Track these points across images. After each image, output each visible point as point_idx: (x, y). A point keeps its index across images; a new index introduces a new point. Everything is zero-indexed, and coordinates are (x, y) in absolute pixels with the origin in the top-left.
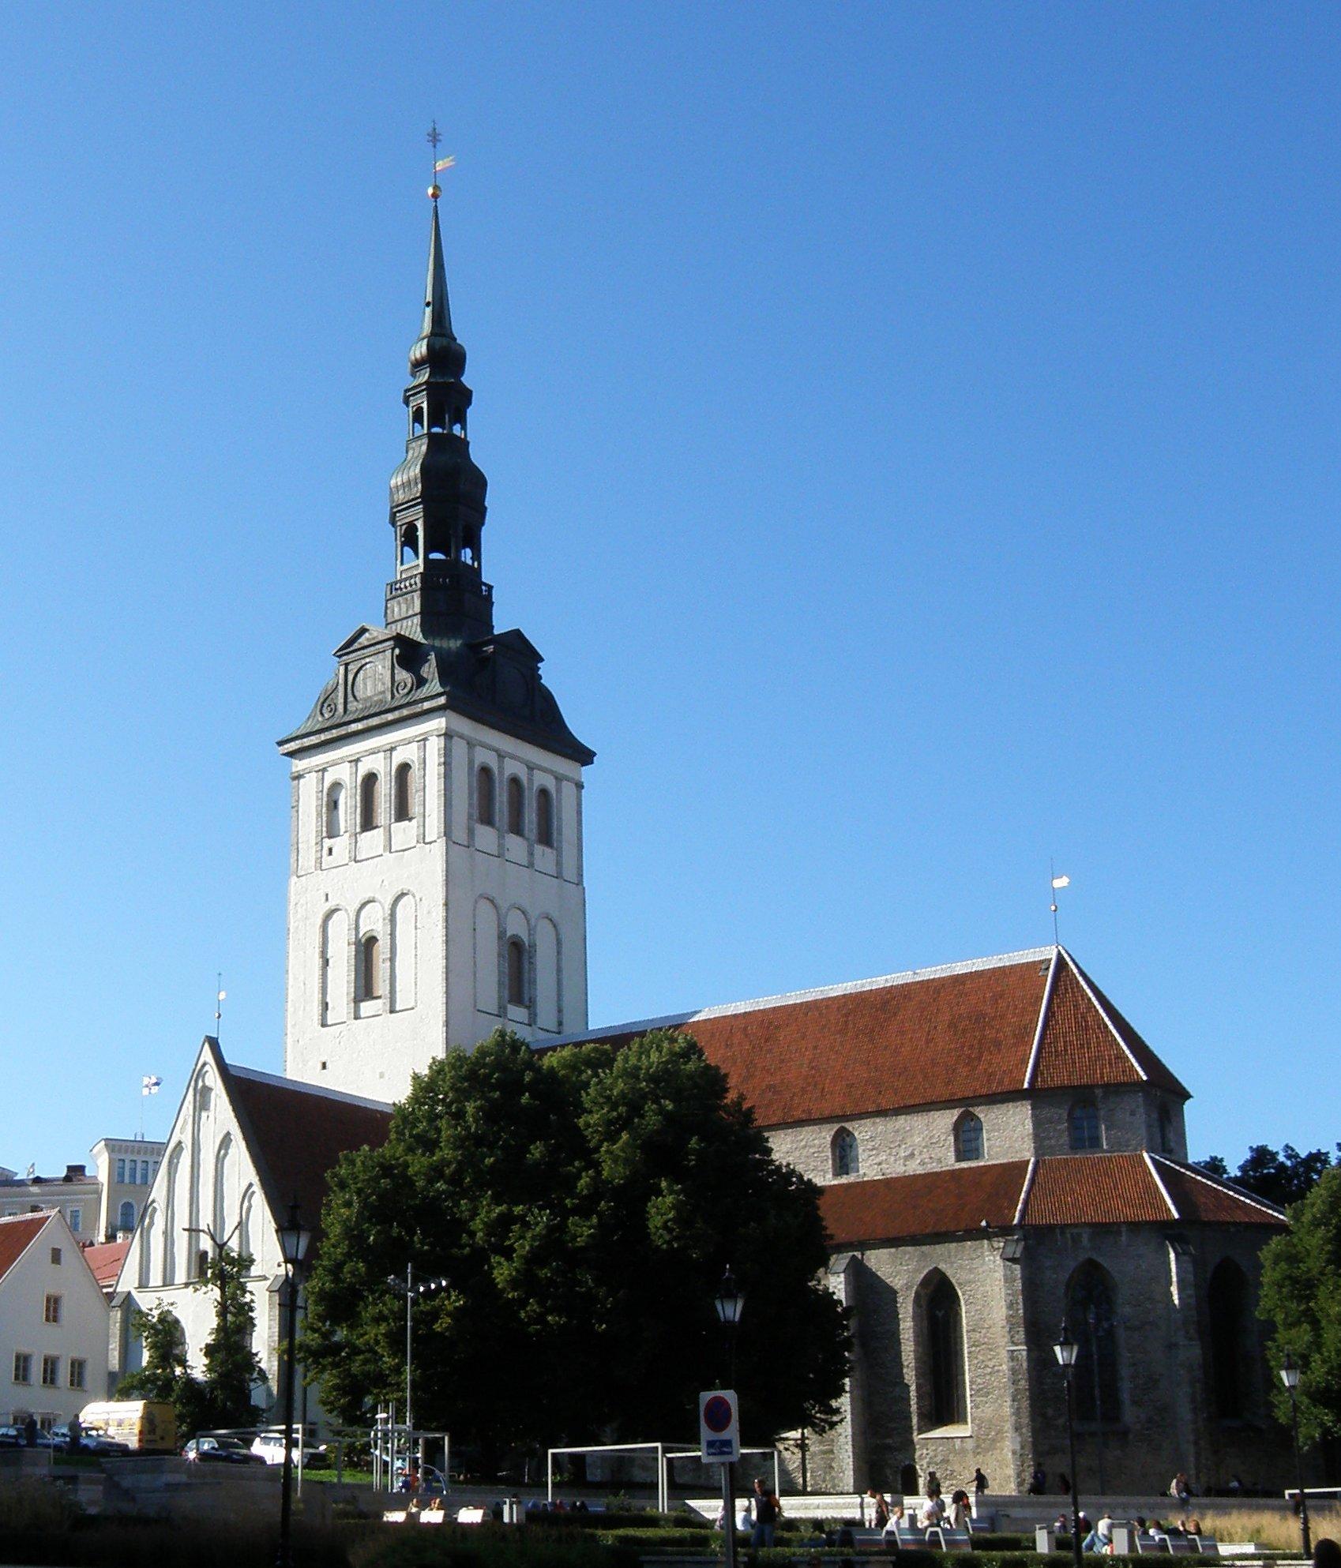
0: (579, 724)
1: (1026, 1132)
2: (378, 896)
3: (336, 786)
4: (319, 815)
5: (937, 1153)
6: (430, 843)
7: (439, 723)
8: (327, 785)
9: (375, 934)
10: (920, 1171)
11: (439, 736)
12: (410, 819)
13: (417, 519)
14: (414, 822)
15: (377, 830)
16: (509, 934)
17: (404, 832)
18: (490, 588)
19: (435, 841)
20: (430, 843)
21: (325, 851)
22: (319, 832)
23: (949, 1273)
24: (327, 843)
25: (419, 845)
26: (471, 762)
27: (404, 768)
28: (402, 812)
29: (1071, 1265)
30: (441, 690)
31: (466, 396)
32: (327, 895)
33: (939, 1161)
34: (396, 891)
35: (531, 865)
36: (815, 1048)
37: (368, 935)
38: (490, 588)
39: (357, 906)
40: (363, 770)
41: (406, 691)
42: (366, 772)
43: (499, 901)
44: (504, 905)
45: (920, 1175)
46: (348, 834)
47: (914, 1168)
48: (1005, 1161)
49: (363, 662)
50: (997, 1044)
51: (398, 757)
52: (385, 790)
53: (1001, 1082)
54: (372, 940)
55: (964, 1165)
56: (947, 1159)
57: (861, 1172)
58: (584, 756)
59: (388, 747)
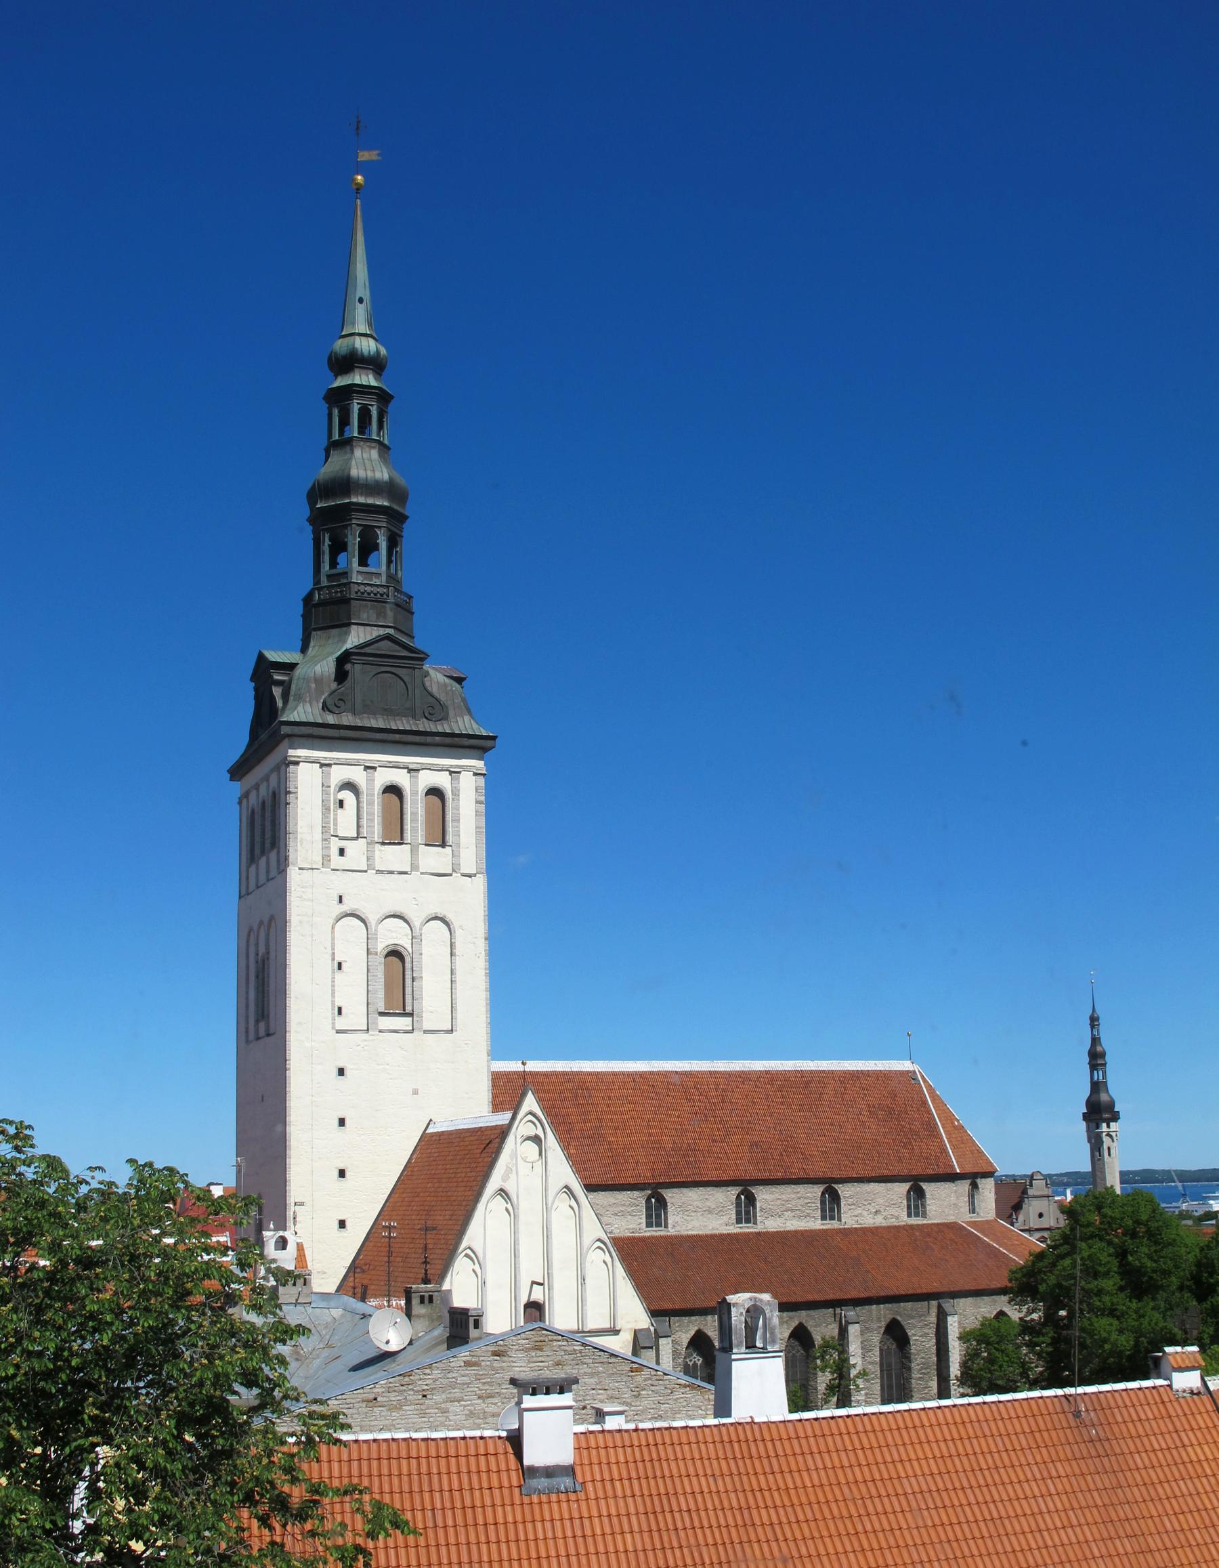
3: (350, 786)
5: (894, 1211)
6: (470, 876)
9: (402, 950)
10: (884, 1223)
13: (379, 527)
14: (448, 849)
20: (470, 876)
21: (334, 852)
22: (325, 829)
25: (454, 874)
28: (439, 837)
32: (341, 897)
33: (897, 1218)
37: (389, 949)
42: (389, 784)
47: (879, 1221)
49: (384, 669)
51: (428, 779)
54: (395, 954)
57: (843, 1220)
59: (418, 766)
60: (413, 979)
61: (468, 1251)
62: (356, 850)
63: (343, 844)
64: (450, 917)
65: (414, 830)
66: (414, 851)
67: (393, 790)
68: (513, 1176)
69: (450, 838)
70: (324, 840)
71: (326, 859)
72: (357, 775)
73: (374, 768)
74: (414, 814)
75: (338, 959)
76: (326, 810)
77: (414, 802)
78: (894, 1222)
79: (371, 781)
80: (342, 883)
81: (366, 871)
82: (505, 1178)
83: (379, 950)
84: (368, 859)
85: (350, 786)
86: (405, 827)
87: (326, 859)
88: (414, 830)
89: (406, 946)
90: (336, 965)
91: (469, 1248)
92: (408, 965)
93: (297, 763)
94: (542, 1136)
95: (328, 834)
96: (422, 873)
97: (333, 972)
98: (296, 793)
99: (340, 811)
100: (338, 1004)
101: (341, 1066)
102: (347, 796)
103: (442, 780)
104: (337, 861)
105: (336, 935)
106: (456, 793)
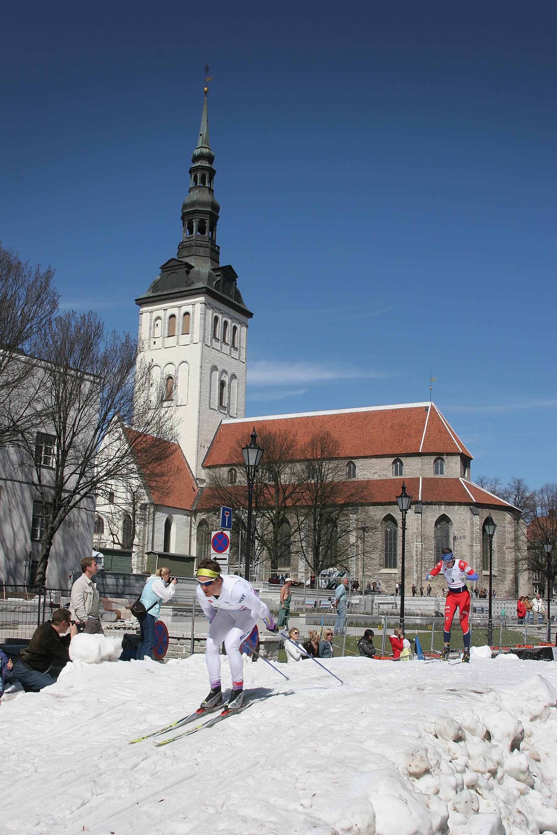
0: (248, 304)
1: (418, 468)
2: (174, 362)
3: (159, 318)
4: (150, 328)
6: (196, 343)
7: (202, 299)
8: (154, 318)
10: (379, 478)
12: (188, 334)
16: (222, 379)
17: (185, 339)
18: (219, 248)
20: (196, 343)
21: (153, 343)
23: (394, 516)
24: (153, 340)
26: (212, 314)
27: (187, 314)
29: (438, 516)
30: (203, 286)
31: (212, 173)
33: (386, 475)
34: (182, 360)
35: (230, 354)
36: (340, 431)
38: (219, 248)
39: (165, 364)
40: (170, 312)
41: (189, 284)
43: (219, 368)
44: (220, 368)
45: (379, 480)
47: (376, 477)
48: (410, 477)
50: (410, 435)
51: (184, 309)
52: (179, 321)
53: (411, 449)
55: (396, 477)
56: (390, 475)
58: (249, 315)
59: (181, 305)
63: (155, 340)
64: (188, 361)
65: (179, 329)
66: (178, 336)
69: (190, 331)
71: (149, 346)
72: (161, 313)
73: (167, 309)
77: (179, 319)
78: (384, 478)
79: (165, 314)
85: (159, 318)
87: (149, 346)
88: (179, 329)
93: (142, 314)
102: (159, 322)
103: (189, 309)
104: (153, 347)
106: (194, 313)
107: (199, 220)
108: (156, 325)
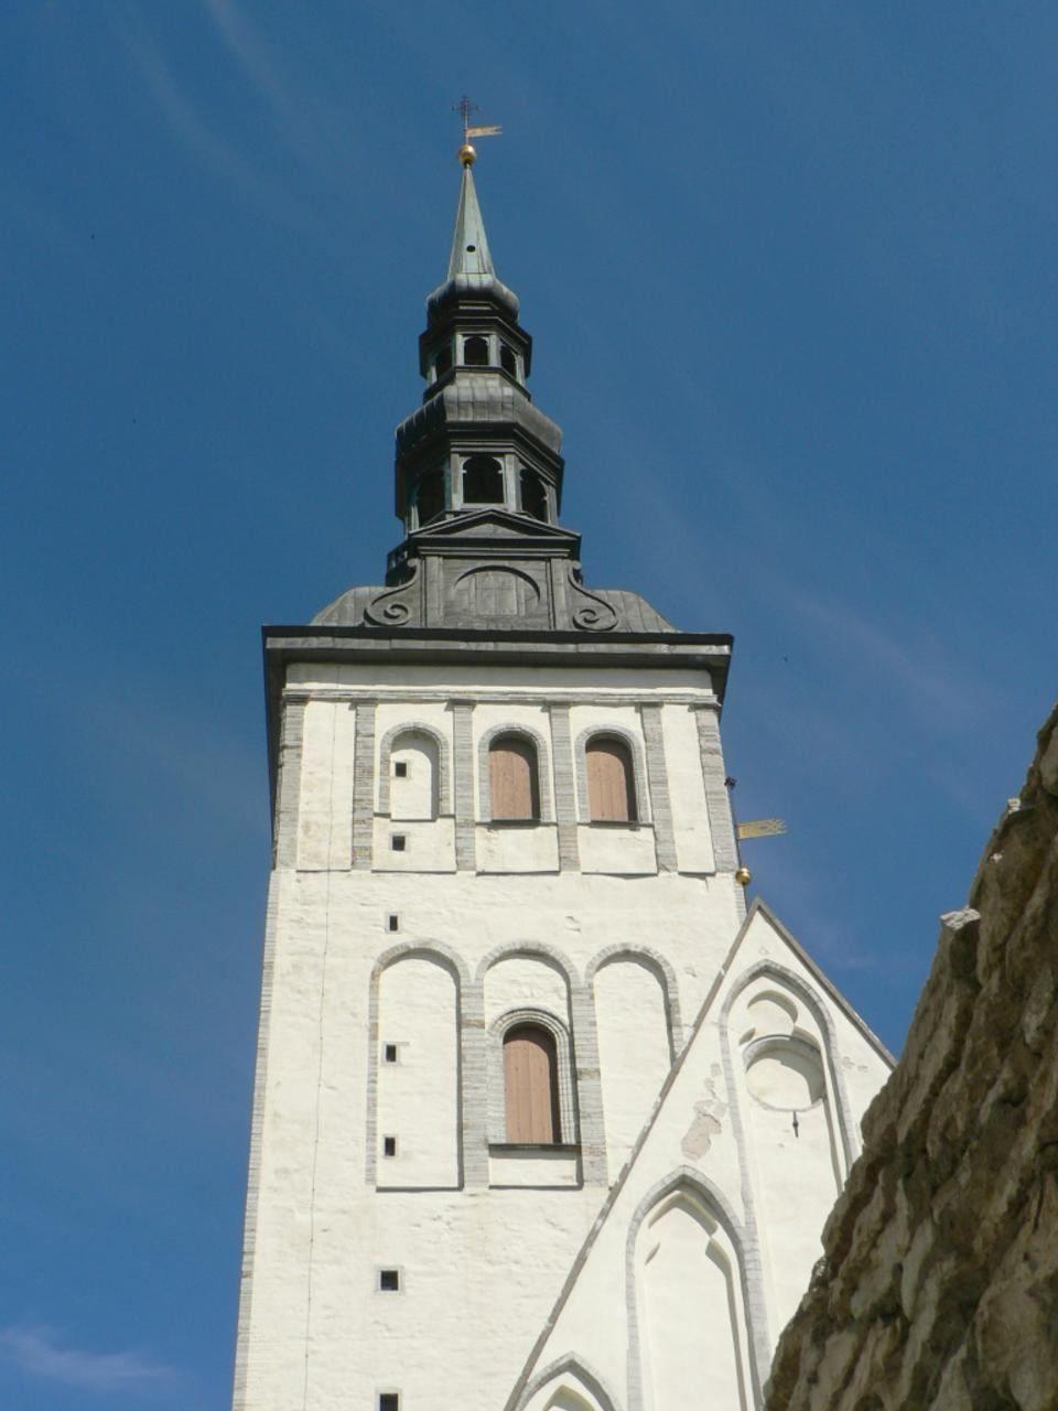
3: (418, 737)
6: (702, 876)
11: (695, 707)
13: (502, 455)
14: (645, 834)
15: (540, 830)
19: (712, 875)
20: (702, 876)
22: (359, 803)
25: (663, 874)
27: (608, 743)
37: (515, 1019)
46: (451, 821)
51: (585, 720)
54: (529, 1030)
59: (569, 698)
60: (575, 1076)
61: (569, 1381)
62: (430, 842)
64: (659, 950)
65: (564, 800)
67: (514, 742)
68: (722, 1143)
69: (646, 812)
70: (354, 822)
72: (435, 718)
74: (562, 777)
75: (385, 1038)
76: (362, 772)
79: (462, 727)
80: (391, 895)
81: (454, 873)
82: (697, 1141)
83: (488, 1019)
84: (458, 851)
85: (418, 737)
86: (543, 797)
87: (360, 854)
89: (556, 1012)
90: (381, 1052)
91: (573, 1367)
92: (562, 1050)
93: (302, 700)
94: (815, 1032)
95: (364, 812)
96: (584, 873)
97: (373, 1061)
98: (299, 747)
99: (397, 784)
100: (383, 1131)
101: (389, 1265)
103: (624, 720)
105: (383, 992)
106: (655, 741)
107: (522, 467)
108: (393, 768)
